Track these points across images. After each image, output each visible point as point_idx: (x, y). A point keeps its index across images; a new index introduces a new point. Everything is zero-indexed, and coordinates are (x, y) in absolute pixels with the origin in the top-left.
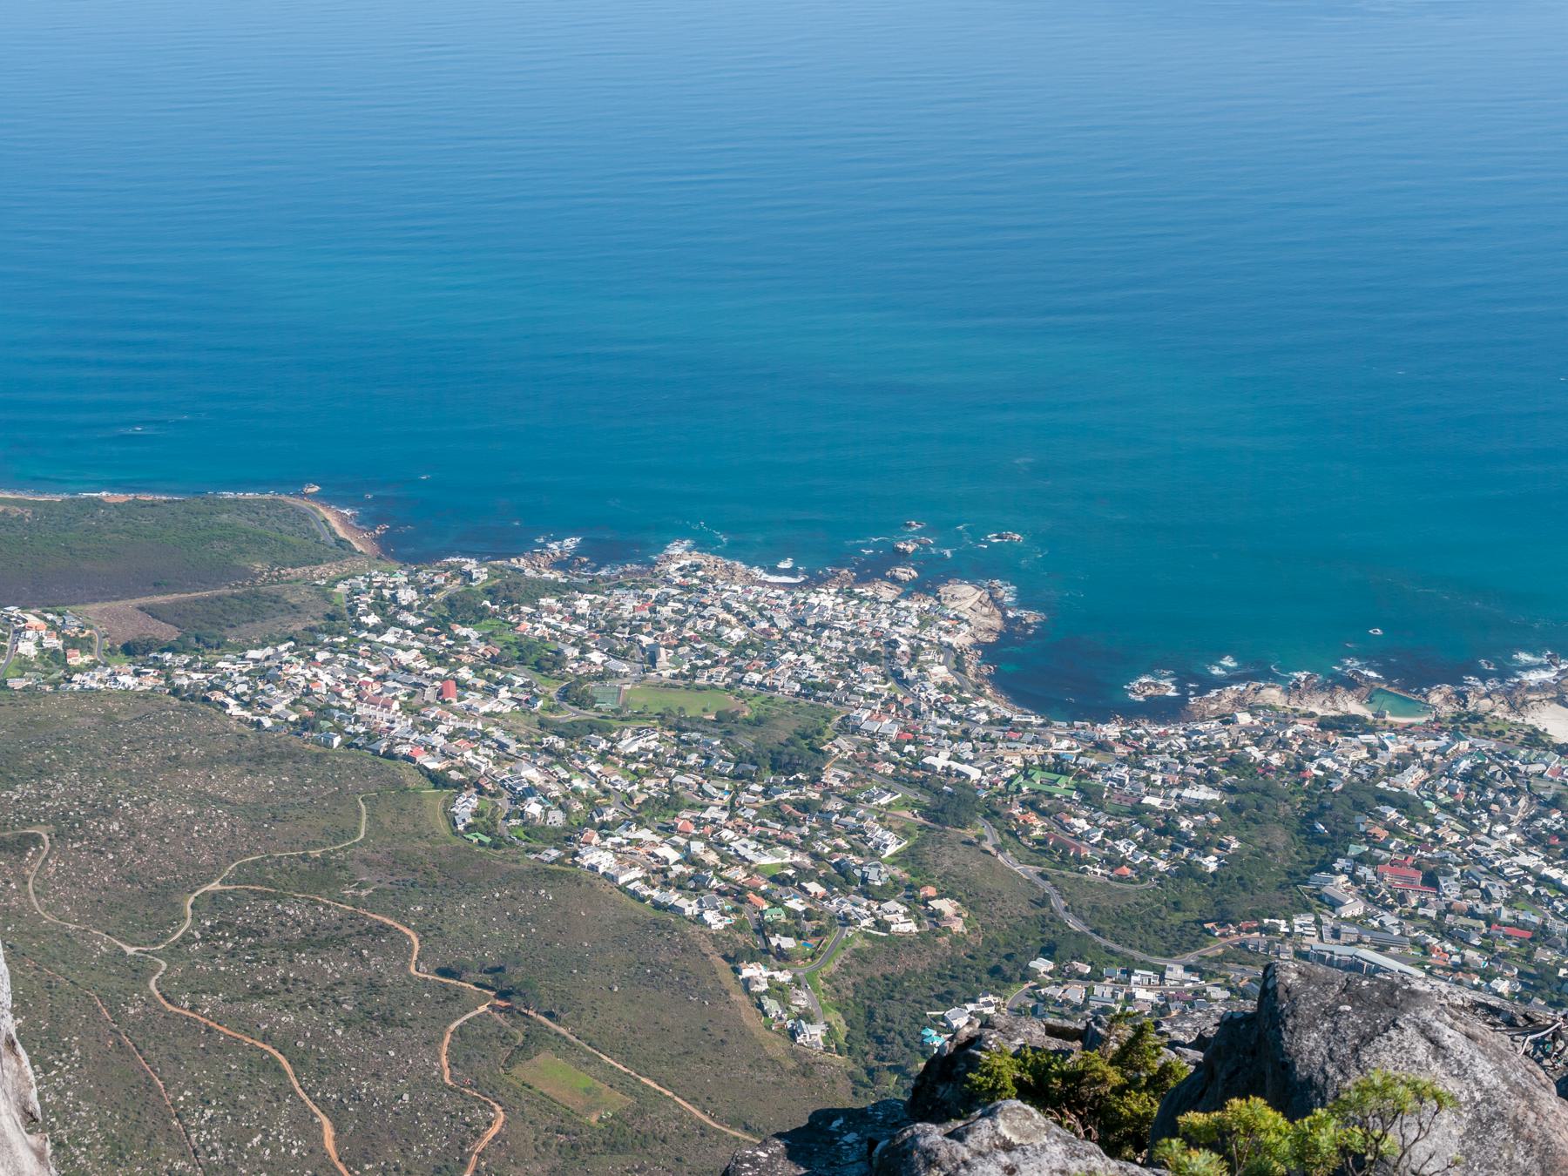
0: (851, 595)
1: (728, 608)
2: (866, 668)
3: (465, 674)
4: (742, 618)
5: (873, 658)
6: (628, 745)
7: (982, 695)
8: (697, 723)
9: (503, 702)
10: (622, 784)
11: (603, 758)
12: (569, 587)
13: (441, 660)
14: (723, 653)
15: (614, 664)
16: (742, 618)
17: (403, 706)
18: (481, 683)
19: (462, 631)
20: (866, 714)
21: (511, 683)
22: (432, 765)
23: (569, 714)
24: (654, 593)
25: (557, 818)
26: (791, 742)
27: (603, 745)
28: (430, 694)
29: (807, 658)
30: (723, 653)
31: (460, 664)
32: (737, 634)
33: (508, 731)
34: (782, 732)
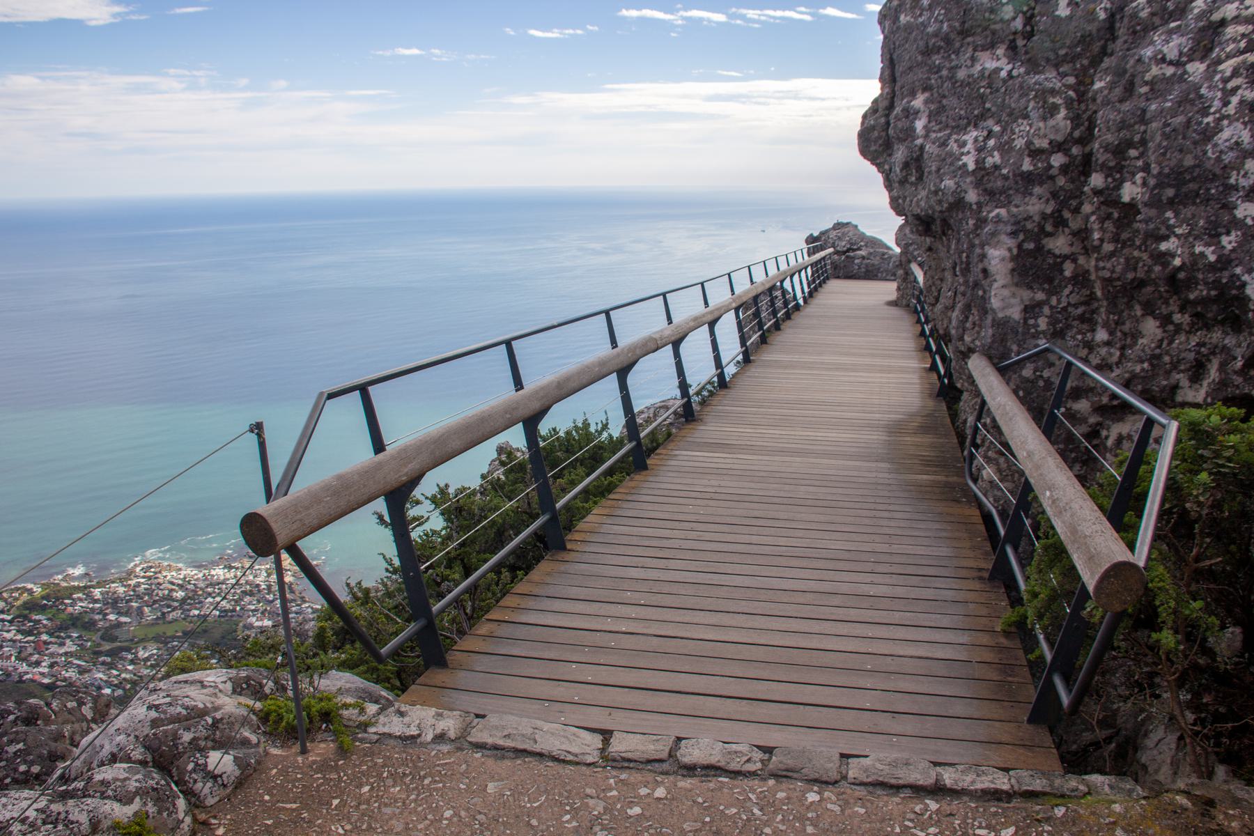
0: (230, 568)
1: (172, 583)
2: (247, 599)
3: (45, 637)
4: (181, 586)
5: (251, 594)
6: (142, 654)
7: (305, 602)
8: (174, 638)
9: (70, 647)
10: (146, 672)
11: (132, 662)
12: (86, 587)
13: (30, 633)
14: (176, 604)
15: (123, 619)
16: (181, 586)
17: (18, 658)
18: (53, 640)
19: (37, 617)
20: (254, 619)
21: (70, 637)
22: (46, 681)
23: (107, 646)
24: (132, 583)
25: (120, 692)
26: (223, 638)
27: (130, 657)
28: (30, 650)
29: (218, 599)
30: (176, 604)
31: (40, 633)
32: (180, 594)
33: (79, 658)
34: (217, 634)
